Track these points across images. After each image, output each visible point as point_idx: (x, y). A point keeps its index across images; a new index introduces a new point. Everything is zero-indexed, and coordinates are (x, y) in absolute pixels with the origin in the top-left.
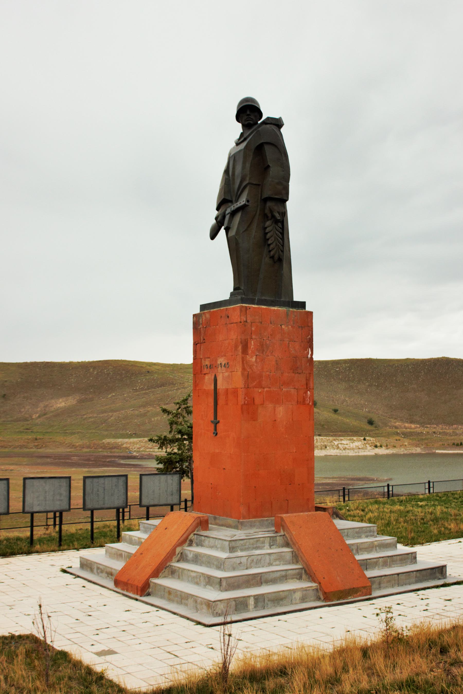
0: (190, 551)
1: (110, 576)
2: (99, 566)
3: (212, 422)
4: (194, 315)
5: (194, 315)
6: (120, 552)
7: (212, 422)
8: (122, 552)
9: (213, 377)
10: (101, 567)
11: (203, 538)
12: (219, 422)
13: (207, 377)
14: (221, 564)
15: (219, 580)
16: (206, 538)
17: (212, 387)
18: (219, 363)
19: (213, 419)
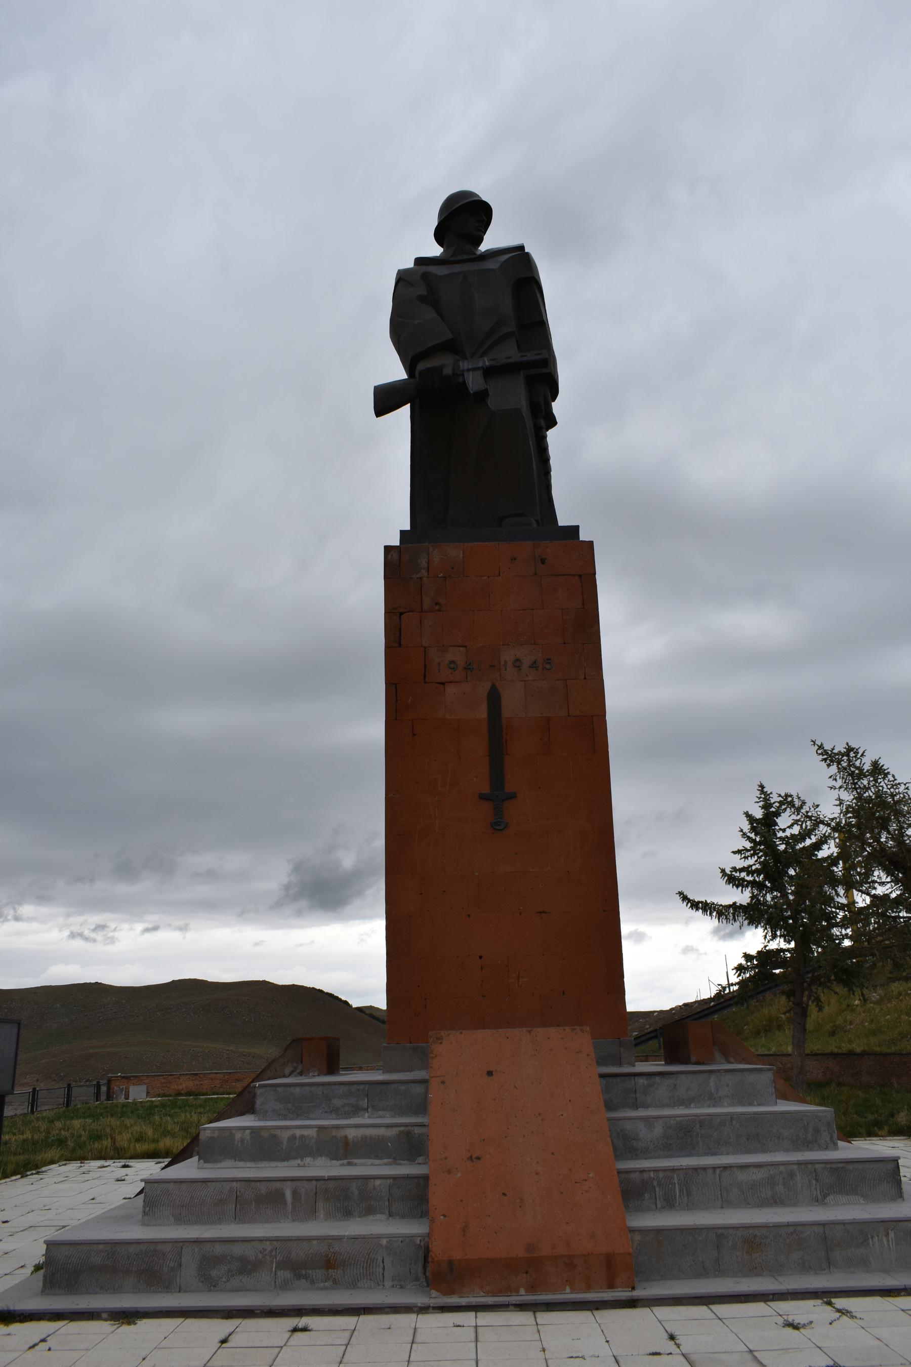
0: (646, 1119)
1: (319, 1273)
2: (219, 1249)
3: (483, 797)
4: (388, 549)
5: (388, 549)
6: (263, 1188)
7: (483, 797)
8: (278, 1185)
9: (484, 688)
10: (238, 1250)
11: (641, 1081)
12: (513, 796)
13: (451, 690)
14: (817, 1131)
15: (891, 1166)
16: (658, 1079)
17: (482, 713)
18: (508, 656)
19: (486, 789)
